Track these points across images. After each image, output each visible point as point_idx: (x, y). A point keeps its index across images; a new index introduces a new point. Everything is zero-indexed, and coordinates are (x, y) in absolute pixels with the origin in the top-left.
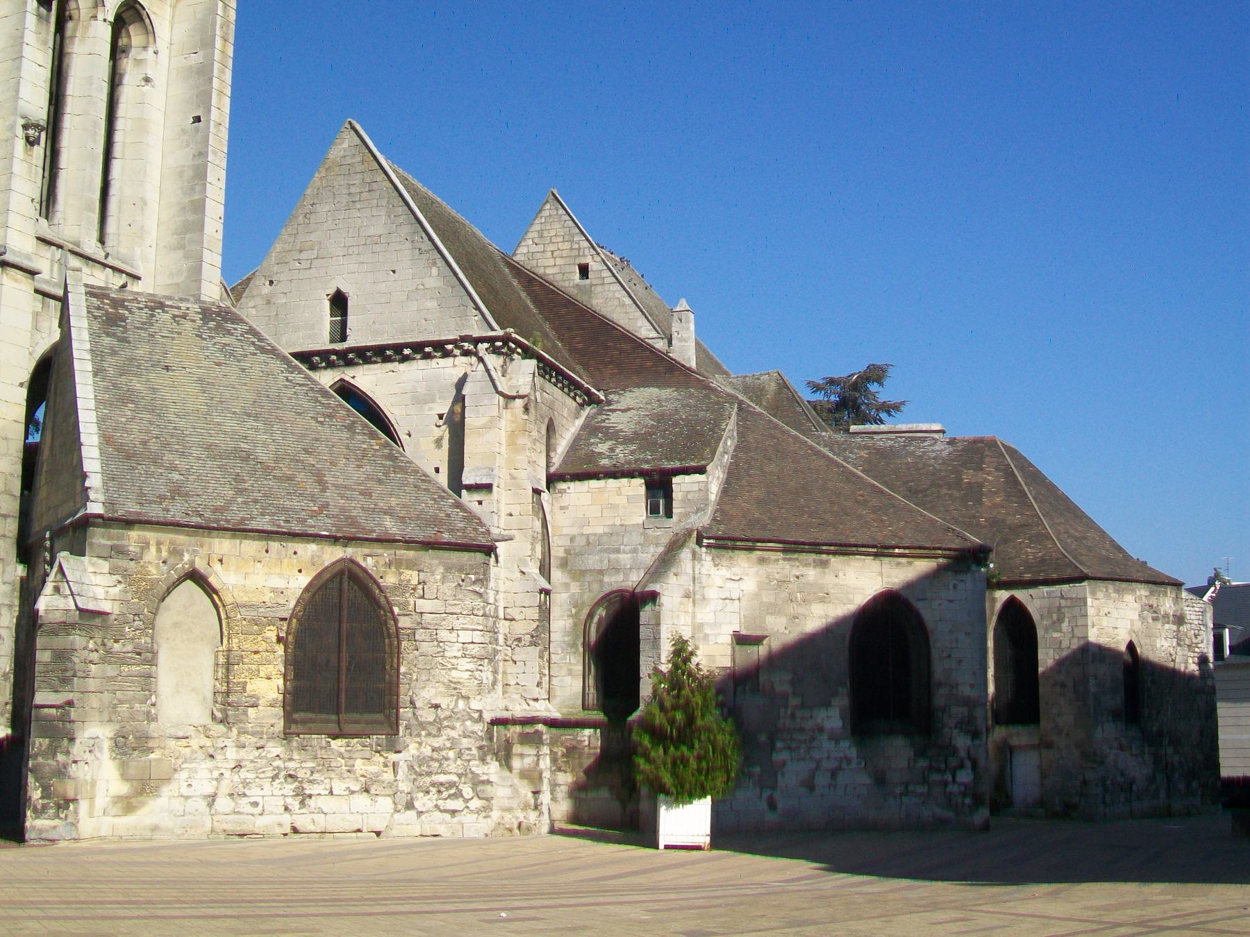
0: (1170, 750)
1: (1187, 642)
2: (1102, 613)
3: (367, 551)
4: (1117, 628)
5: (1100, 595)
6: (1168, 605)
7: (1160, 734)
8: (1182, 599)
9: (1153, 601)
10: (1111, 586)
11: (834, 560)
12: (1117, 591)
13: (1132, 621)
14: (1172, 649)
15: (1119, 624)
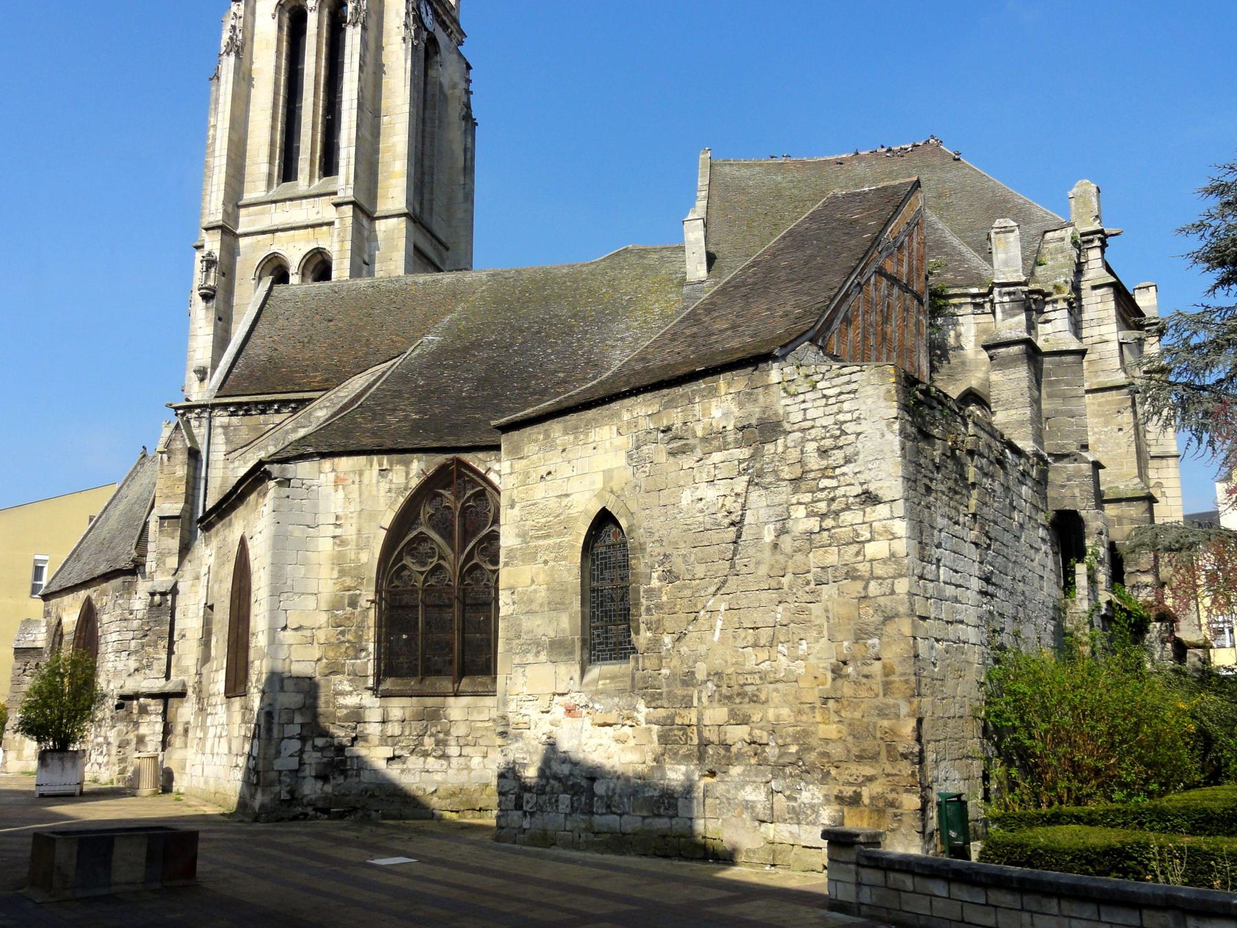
0: (716, 714)
1: (786, 473)
2: (535, 476)
3: (94, 588)
4: (567, 495)
5: (530, 449)
6: (716, 413)
7: (688, 679)
8: (767, 387)
9: (675, 418)
10: (556, 427)
11: (233, 514)
12: (575, 430)
13: (608, 475)
14: (729, 502)
15: (574, 486)
